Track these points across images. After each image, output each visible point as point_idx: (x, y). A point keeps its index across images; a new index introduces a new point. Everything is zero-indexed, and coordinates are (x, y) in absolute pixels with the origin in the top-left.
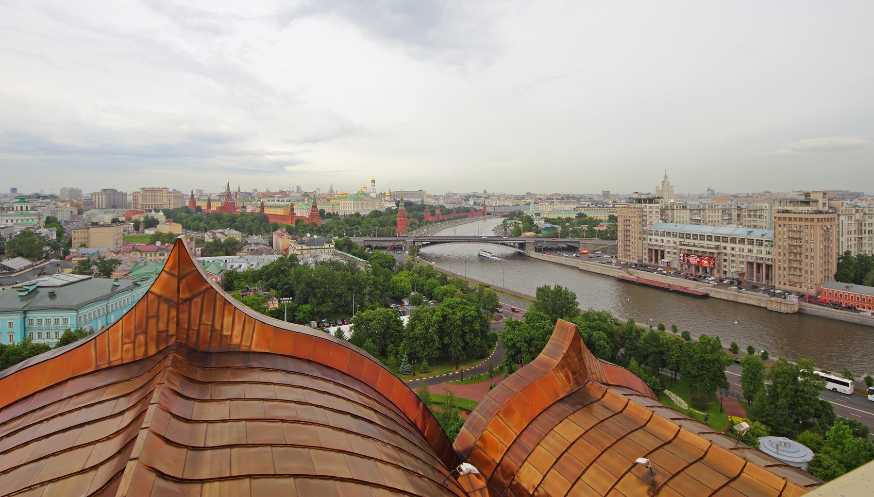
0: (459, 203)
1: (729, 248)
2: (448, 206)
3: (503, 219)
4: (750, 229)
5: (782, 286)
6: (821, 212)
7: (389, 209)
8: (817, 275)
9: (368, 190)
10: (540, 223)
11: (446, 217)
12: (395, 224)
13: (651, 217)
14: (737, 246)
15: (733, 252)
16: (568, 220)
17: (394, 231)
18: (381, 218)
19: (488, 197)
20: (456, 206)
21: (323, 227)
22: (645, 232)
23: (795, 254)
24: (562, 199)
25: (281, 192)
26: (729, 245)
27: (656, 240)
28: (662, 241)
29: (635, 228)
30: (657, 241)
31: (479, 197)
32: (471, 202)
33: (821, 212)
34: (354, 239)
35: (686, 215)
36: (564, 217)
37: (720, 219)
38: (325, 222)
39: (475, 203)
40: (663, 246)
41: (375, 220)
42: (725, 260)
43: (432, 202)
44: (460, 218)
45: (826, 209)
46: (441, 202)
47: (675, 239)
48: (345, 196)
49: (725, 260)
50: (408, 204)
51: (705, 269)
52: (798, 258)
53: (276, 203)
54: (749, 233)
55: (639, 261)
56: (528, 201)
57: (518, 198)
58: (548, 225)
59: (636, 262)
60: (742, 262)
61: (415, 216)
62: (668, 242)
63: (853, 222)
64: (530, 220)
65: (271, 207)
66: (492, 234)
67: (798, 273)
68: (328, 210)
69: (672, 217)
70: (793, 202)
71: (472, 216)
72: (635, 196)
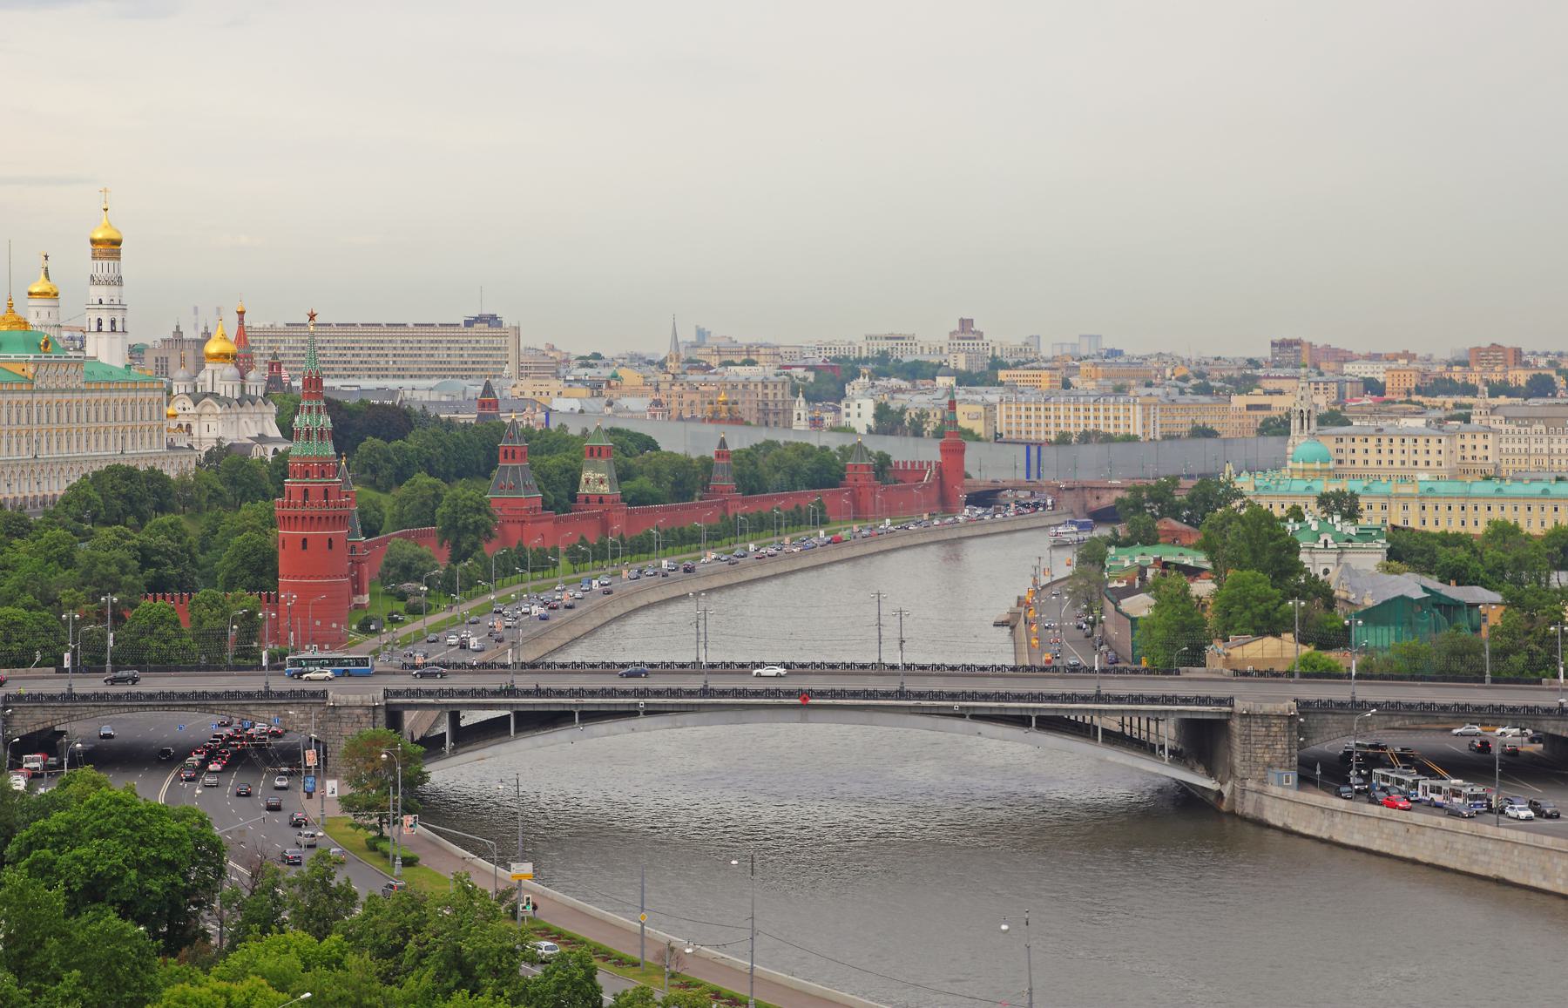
0: (771, 414)
7: (225, 459)
10: (1356, 573)
11: (656, 522)
12: (260, 571)
17: (250, 626)
18: (155, 532)
19: (984, 375)
20: (740, 440)
31: (918, 372)
32: (860, 411)
39: (888, 422)
41: (105, 545)
43: (567, 405)
44: (762, 525)
46: (633, 410)
50: (365, 428)
56: (1279, 404)
57: (1205, 382)
58: (1411, 585)
61: (424, 514)
64: (1267, 550)
66: (999, 650)
71: (859, 512)
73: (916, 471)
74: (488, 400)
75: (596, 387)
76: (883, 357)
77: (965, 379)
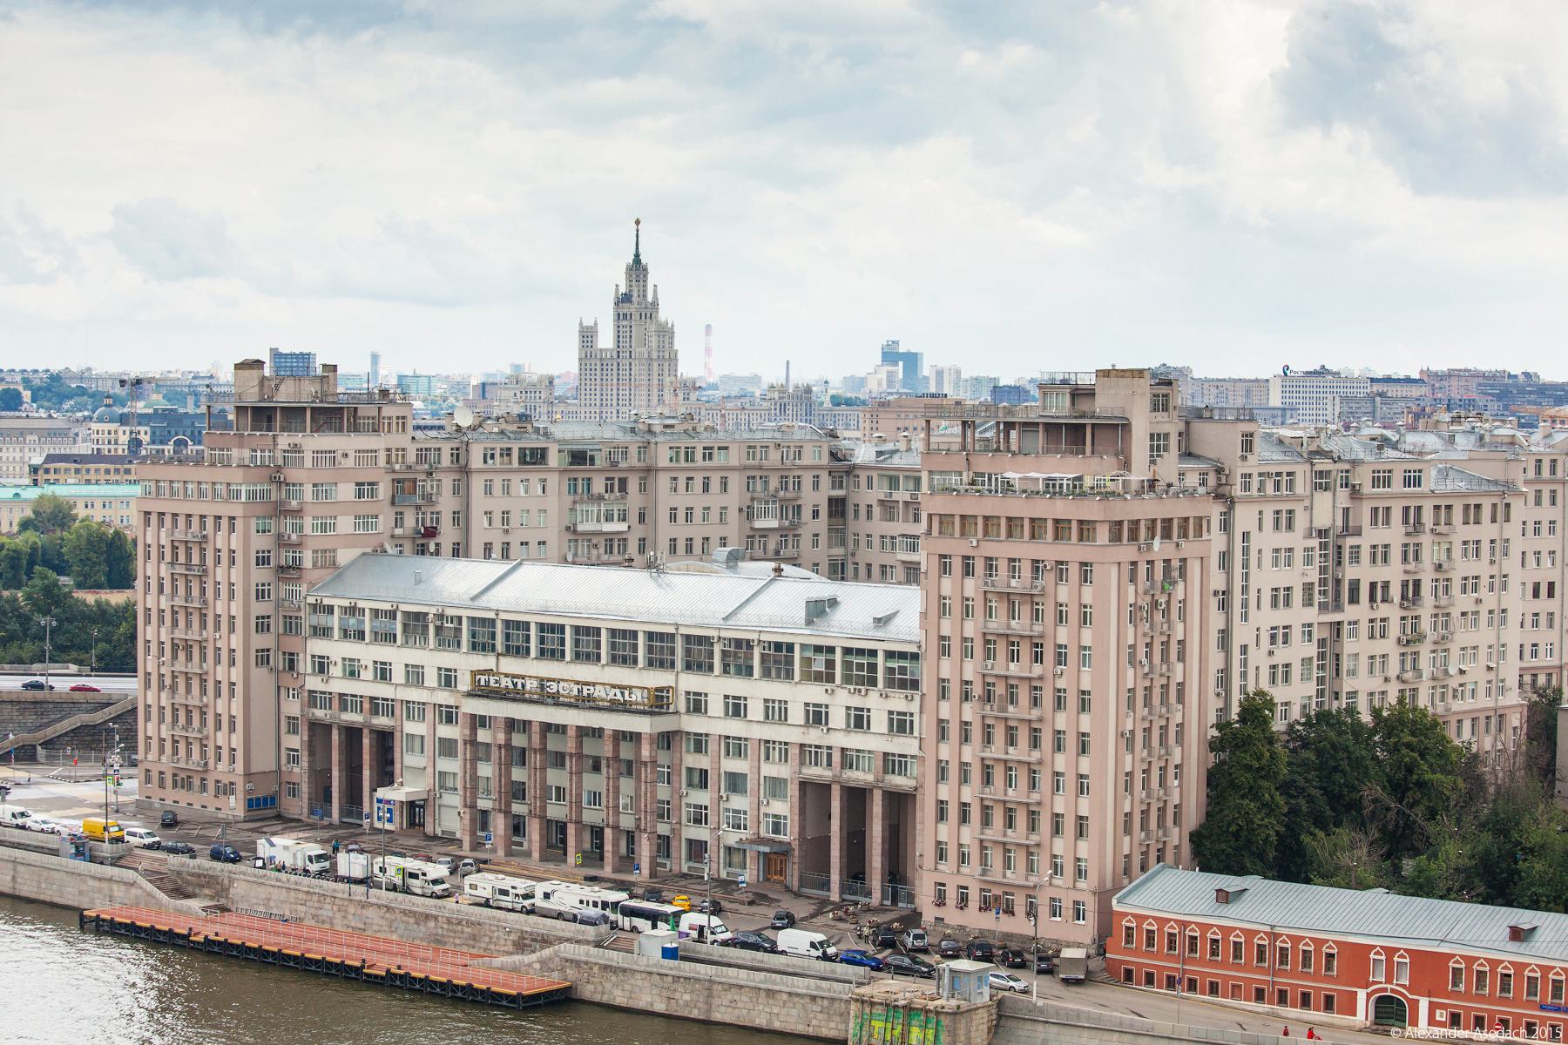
1: (716, 706)
14: (757, 690)
15: (735, 728)
26: (717, 687)
28: (383, 673)
47: (448, 659)
49: (701, 779)
54: (818, 610)
60: (776, 786)
69: (461, 518)
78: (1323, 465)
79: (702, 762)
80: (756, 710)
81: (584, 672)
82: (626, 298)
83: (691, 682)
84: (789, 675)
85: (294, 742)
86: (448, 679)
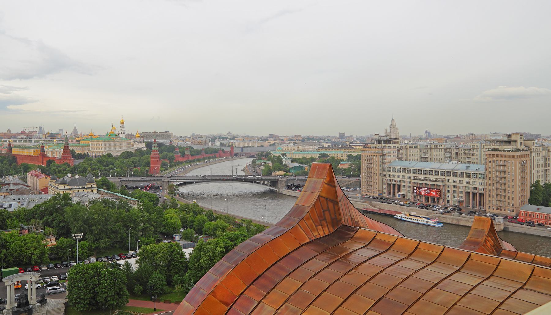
1: (452, 181)
2: (195, 147)
3: (252, 159)
4: (468, 165)
5: (491, 211)
6: (519, 150)
7: (138, 150)
8: (516, 200)
9: (117, 132)
11: (196, 157)
12: (148, 164)
13: (389, 156)
14: (458, 179)
15: (455, 184)
16: (313, 159)
19: (234, 138)
20: (205, 147)
21: (76, 167)
22: (384, 169)
23: (501, 184)
24: (303, 140)
25: (23, 133)
26: (452, 179)
27: (394, 176)
28: (399, 177)
29: (376, 166)
30: (394, 177)
31: (224, 138)
33: (519, 150)
34: (111, 179)
35: (417, 153)
36: (308, 157)
37: (443, 157)
38: (77, 162)
39: (221, 144)
40: (400, 181)
42: (449, 191)
43: (180, 143)
44: (209, 158)
45: (522, 147)
47: (409, 175)
48: (92, 138)
49: (449, 191)
51: (433, 199)
52: (503, 187)
53: (22, 143)
55: (379, 195)
56: (272, 142)
59: (377, 195)
60: (461, 192)
61: (165, 157)
62: (404, 177)
63: (540, 158)
64: (280, 160)
65: (19, 147)
66: (243, 174)
67: (503, 199)
68: (78, 150)
69: (406, 155)
70: (499, 142)
71: (220, 157)
72: (376, 137)
73: (227, 151)
74: (171, 142)
75: (183, 140)
76: (219, 136)
77: (230, 139)
78: (544, 147)
79: (449, 189)
80: (458, 182)
81: (430, 176)
82: (392, 125)
83: (447, 178)
84: (463, 177)
85: (385, 186)
86: (409, 177)
